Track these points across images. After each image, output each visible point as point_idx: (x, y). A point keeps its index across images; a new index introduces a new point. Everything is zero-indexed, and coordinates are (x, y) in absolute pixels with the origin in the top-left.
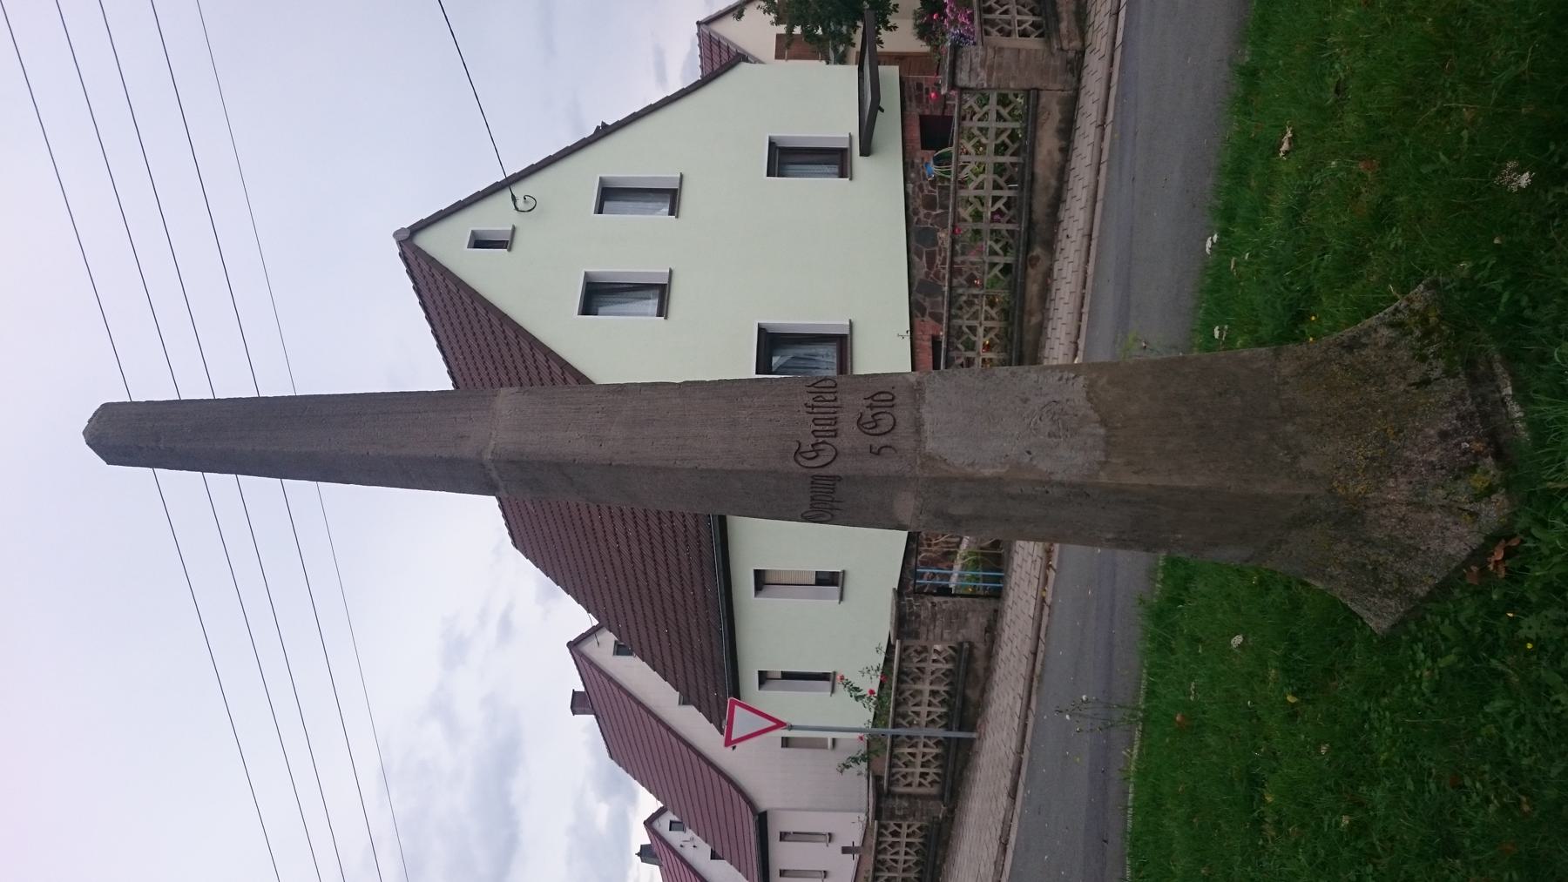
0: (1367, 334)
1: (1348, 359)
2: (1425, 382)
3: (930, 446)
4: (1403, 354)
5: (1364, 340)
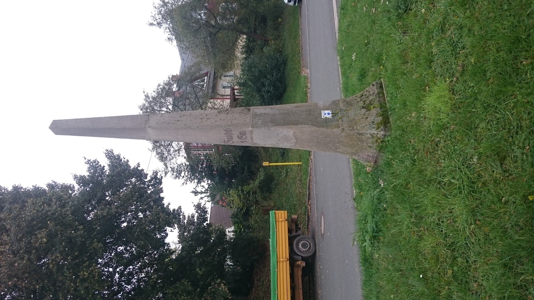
0: (365, 133)
1: (358, 136)
2: (370, 147)
3: (255, 142)
4: (370, 141)
5: (364, 134)
